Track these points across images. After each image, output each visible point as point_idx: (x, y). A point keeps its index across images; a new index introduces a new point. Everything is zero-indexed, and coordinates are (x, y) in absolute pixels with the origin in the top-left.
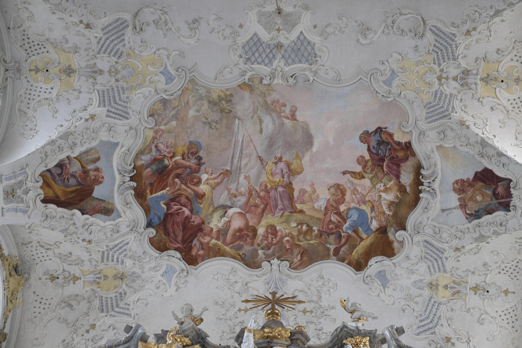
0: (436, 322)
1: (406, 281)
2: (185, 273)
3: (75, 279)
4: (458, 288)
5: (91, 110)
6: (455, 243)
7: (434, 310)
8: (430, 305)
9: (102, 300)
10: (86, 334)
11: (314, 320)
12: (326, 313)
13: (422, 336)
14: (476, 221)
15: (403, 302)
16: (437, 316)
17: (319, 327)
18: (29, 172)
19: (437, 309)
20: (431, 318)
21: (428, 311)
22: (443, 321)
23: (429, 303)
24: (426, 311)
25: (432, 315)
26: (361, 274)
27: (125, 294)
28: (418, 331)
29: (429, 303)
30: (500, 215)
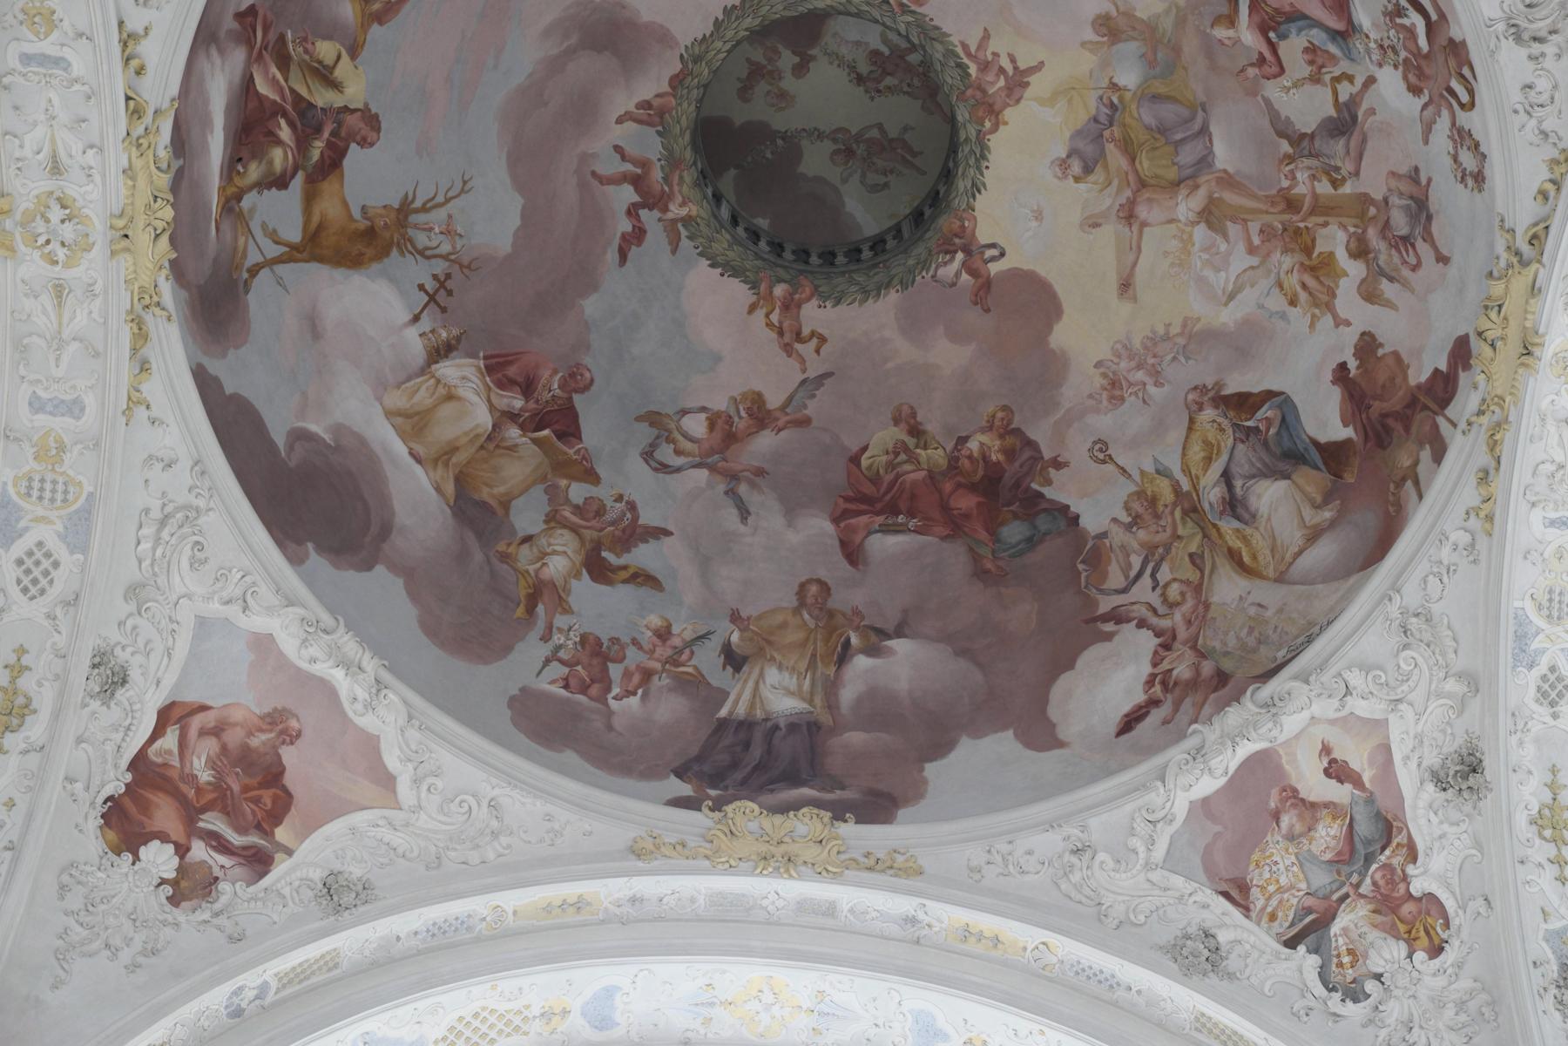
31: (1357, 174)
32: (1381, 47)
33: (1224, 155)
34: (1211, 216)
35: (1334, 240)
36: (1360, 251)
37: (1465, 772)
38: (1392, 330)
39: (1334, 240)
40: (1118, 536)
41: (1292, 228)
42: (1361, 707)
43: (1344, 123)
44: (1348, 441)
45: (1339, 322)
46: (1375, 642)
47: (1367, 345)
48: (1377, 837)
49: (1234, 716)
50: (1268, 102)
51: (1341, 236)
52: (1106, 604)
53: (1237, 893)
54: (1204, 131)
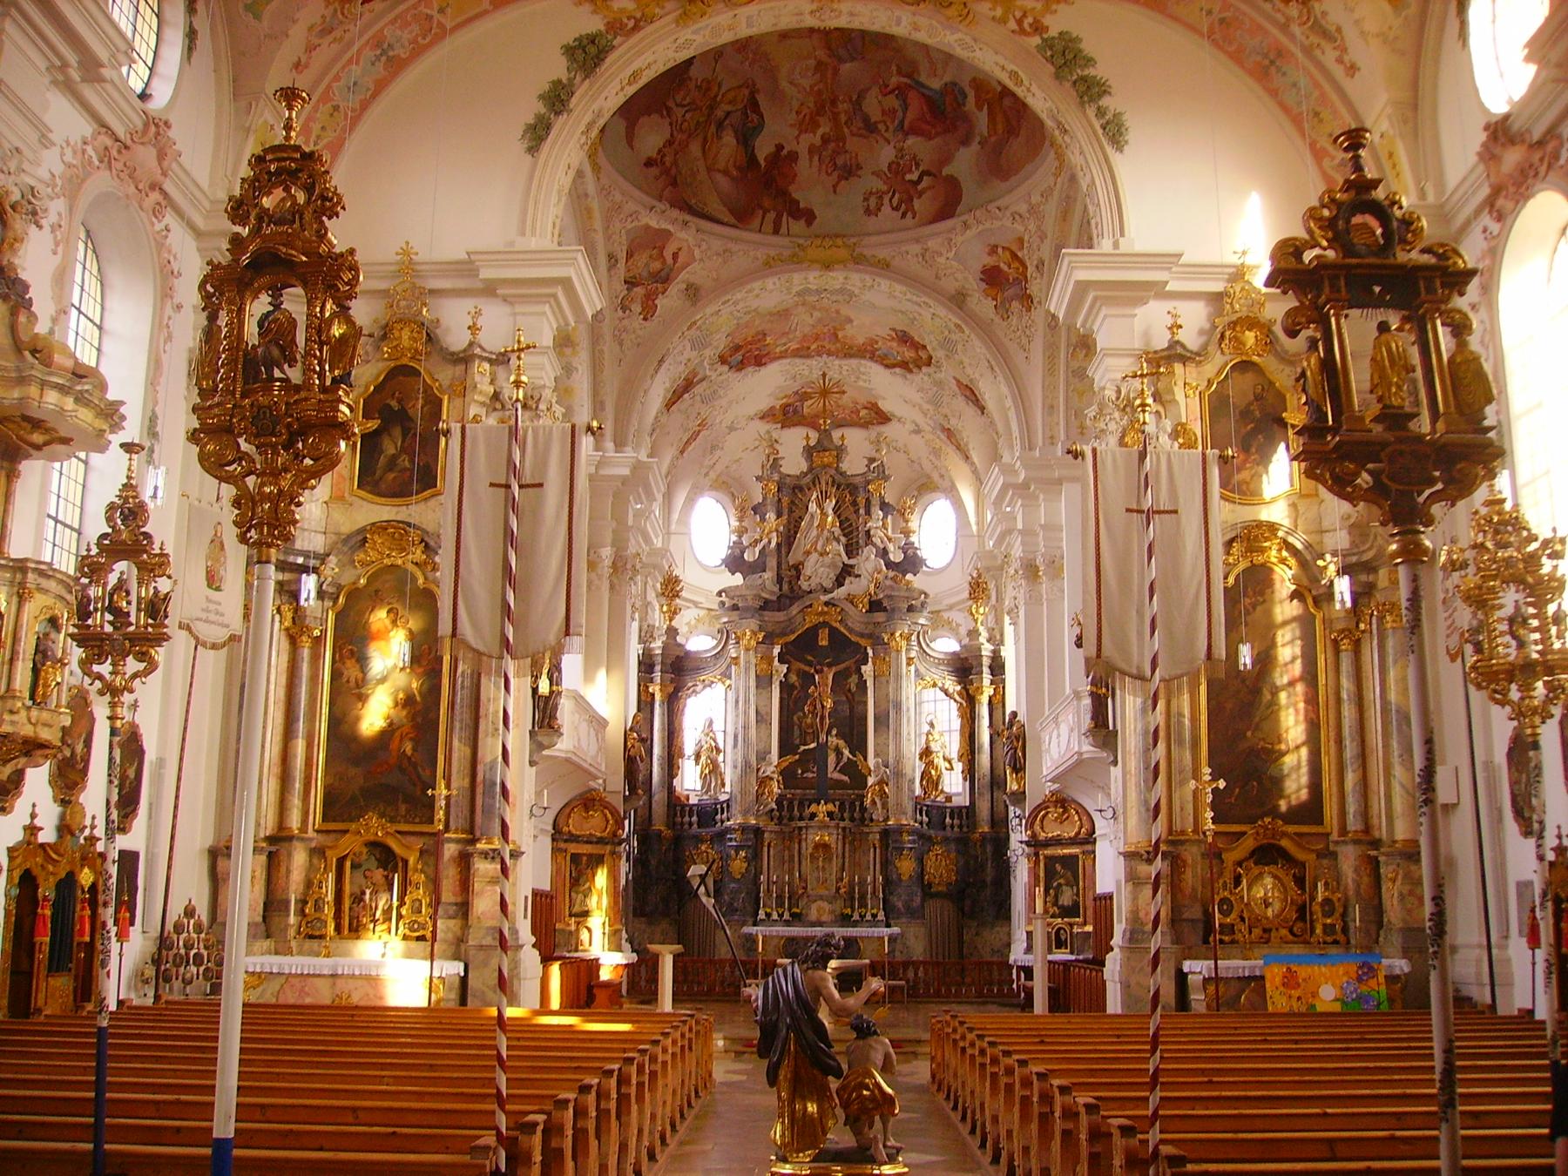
5: (686, 355)
26: (888, 372)
31: (853, 135)
32: (902, 149)
33: (846, 67)
34: (820, 66)
35: (825, 128)
36: (825, 140)
37: (693, 293)
38: (806, 168)
39: (825, 128)
40: (692, 85)
41: (824, 105)
42: (697, 252)
43: (870, 128)
44: (758, 164)
45: (797, 138)
46: (717, 244)
47: (793, 157)
48: (663, 279)
49: (675, 213)
50: (868, 89)
51: (828, 130)
52: (671, 104)
53: (630, 255)
54: (853, 59)
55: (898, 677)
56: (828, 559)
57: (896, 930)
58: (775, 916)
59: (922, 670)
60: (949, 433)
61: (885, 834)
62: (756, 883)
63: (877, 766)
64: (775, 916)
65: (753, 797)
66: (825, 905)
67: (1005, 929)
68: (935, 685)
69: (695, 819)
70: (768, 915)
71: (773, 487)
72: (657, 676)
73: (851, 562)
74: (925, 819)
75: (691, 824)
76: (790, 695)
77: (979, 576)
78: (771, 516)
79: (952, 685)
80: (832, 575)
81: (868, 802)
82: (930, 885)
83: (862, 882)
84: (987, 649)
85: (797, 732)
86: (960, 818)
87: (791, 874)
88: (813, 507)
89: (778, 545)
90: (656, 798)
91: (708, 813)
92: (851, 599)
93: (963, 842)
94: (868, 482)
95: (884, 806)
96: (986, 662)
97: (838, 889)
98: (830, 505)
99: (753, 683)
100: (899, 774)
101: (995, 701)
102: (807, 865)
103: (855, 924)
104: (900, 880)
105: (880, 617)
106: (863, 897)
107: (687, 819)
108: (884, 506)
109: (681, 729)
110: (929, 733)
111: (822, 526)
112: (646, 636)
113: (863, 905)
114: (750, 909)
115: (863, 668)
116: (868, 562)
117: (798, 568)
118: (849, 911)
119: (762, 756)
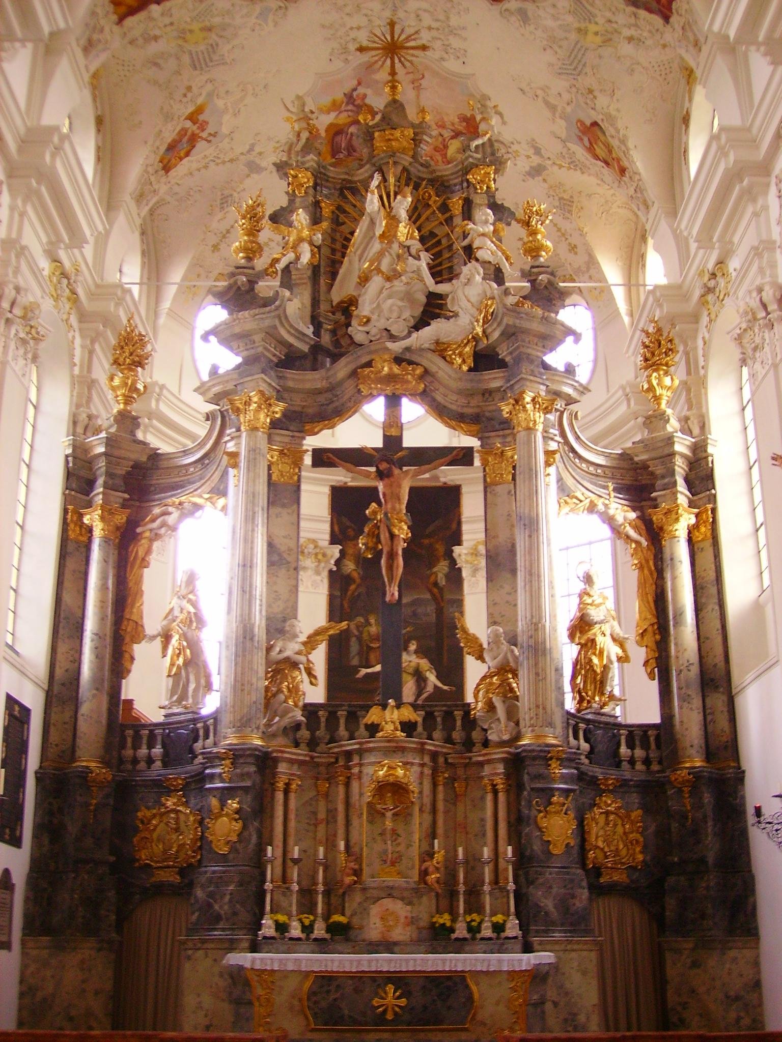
0: (579, 69)
1: (550, 23)
2: (283, 10)
3: (156, 38)
4: (609, 36)
6: (608, 15)
7: (580, 56)
8: (576, 50)
9: (191, 54)
10: (184, 100)
11: (442, 37)
12: (455, 32)
13: (563, 77)
14: (634, 9)
15: (545, 42)
16: (583, 62)
17: (446, 43)
18: (99, 10)
19: (583, 55)
20: (575, 64)
21: (573, 56)
22: (588, 69)
23: (575, 47)
24: (570, 56)
25: (576, 61)
27: (217, 45)
28: (560, 71)
29: (575, 47)
30: (657, 20)
55: (532, 474)
56: (399, 285)
57: (544, 957)
58: (296, 931)
59: (570, 482)
60: (591, 133)
61: (517, 763)
62: (259, 862)
63: (495, 641)
64: (296, 931)
65: (258, 696)
66: (400, 909)
67: (748, 953)
68: (592, 509)
69: (158, 751)
70: (282, 928)
71: (306, 179)
72: (98, 494)
73: (442, 288)
74: (585, 746)
75: (150, 761)
76: (344, 590)
77: (659, 330)
78: (301, 217)
79: (622, 512)
80: (407, 314)
81: (478, 709)
82: (597, 871)
83: (473, 862)
84: (682, 445)
85: (354, 647)
86: (645, 746)
87: (331, 845)
88: (372, 202)
89: (315, 269)
90: (84, 709)
91: (181, 739)
92: (440, 349)
93: (653, 792)
94: (467, 170)
95: (512, 714)
96: (680, 467)
97: (424, 873)
98: (403, 204)
99: (262, 487)
100: (539, 650)
101: (698, 536)
102: (361, 829)
103: (460, 946)
104: (549, 854)
105: (494, 379)
106: (474, 893)
107: (143, 751)
108: (496, 208)
109: (139, 593)
110: (584, 594)
111: (388, 236)
112: (81, 425)
113: (474, 905)
114: (245, 916)
115: (457, 550)
116: (470, 291)
117: (347, 308)
118: (445, 919)
119: (279, 626)
